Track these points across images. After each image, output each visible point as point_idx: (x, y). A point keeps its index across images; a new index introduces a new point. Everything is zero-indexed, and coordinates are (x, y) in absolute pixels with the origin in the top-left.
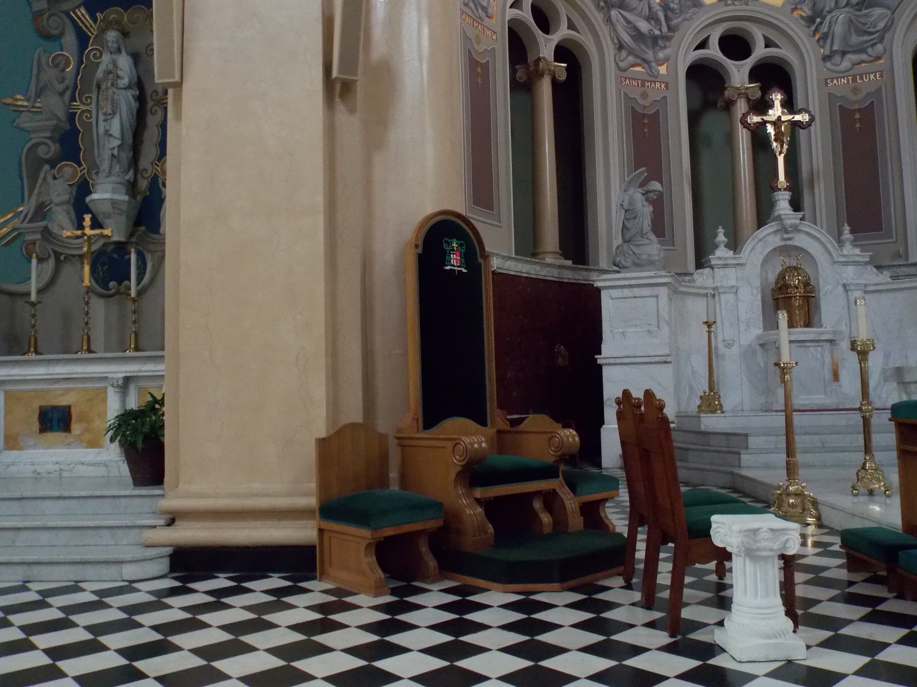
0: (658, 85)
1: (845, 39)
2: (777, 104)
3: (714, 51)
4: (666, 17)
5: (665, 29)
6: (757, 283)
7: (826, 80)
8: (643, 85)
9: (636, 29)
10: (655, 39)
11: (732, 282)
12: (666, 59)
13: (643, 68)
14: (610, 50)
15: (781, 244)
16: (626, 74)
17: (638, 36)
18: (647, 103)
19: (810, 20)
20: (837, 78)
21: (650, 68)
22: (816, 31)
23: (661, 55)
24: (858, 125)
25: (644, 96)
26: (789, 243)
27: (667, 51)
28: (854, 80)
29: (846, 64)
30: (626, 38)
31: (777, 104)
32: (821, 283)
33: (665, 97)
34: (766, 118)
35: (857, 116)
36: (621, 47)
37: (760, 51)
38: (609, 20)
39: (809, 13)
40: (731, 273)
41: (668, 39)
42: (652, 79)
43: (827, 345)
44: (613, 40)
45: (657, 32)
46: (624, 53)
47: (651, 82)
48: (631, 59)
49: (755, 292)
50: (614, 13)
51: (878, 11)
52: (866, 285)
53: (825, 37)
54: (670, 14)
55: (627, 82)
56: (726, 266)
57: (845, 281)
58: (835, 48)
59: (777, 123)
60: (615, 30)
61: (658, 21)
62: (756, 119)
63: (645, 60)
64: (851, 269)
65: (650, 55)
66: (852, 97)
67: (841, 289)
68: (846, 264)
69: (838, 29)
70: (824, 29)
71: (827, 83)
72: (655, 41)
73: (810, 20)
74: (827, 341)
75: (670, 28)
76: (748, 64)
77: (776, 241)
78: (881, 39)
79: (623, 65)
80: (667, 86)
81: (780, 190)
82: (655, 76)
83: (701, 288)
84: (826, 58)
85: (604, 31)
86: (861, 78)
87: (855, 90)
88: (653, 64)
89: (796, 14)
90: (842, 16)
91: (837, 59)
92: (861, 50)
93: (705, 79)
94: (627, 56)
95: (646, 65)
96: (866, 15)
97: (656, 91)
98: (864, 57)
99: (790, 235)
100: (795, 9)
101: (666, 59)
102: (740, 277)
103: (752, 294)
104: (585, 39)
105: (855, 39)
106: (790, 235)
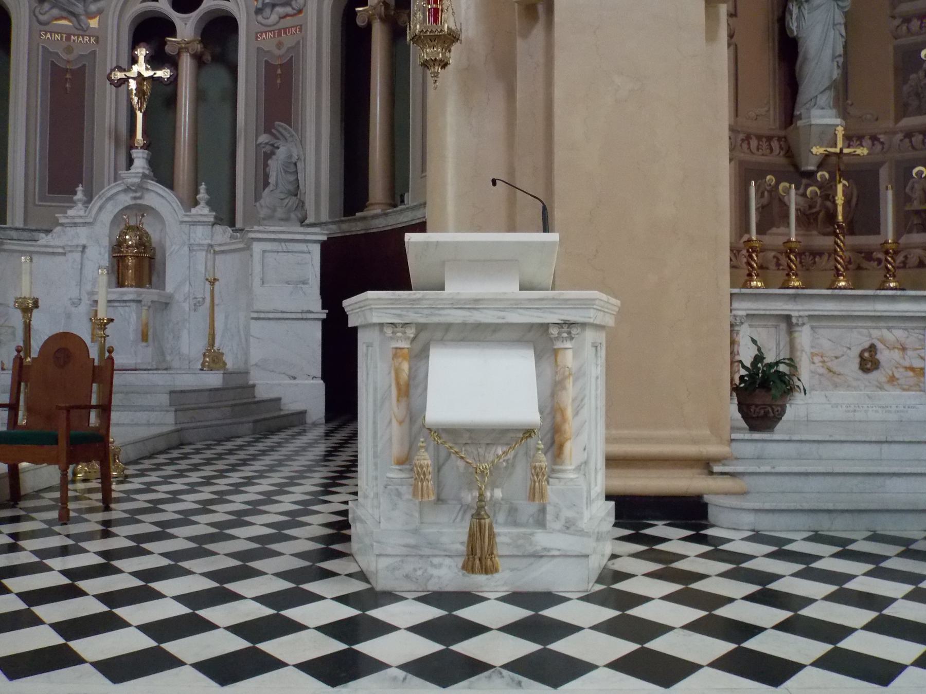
0: (86, 39)
2: (141, 59)
6: (105, 242)
7: (257, 33)
8: (68, 38)
11: (83, 241)
12: (100, 12)
13: (70, 21)
15: (132, 202)
16: (47, 28)
18: (71, 57)
20: (265, 32)
21: (79, 21)
23: (93, 8)
24: (279, 81)
25: (69, 50)
26: (139, 202)
28: (279, 35)
29: (274, 18)
31: (141, 59)
32: (168, 244)
33: (94, 52)
34: (128, 74)
35: (279, 72)
40: (83, 231)
42: (81, 32)
43: (133, 305)
47: (78, 36)
48: (55, 12)
49: (103, 251)
52: (211, 246)
55: (48, 35)
56: (75, 225)
57: (192, 241)
59: (140, 78)
62: (119, 75)
64: (200, 230)
66: (277, 52)
67: (186, 248)
68: (194, 223)
71: (257, 37)
74: (133, 301)
77: (126, 200)
79: (43, 18)
80: (97, 41)
81: (137, 148)
82: (83, 30)
83: (46, 246)
86: (285, 33)
87: (279, 45)
88: (83, 17)
94: (51, 8)
95: (74, 19)
97: (82, 43)
98: (289, 10)
99: (138, 194)
101: (100, 12)
103: (100, 254)
106: (138, 194)
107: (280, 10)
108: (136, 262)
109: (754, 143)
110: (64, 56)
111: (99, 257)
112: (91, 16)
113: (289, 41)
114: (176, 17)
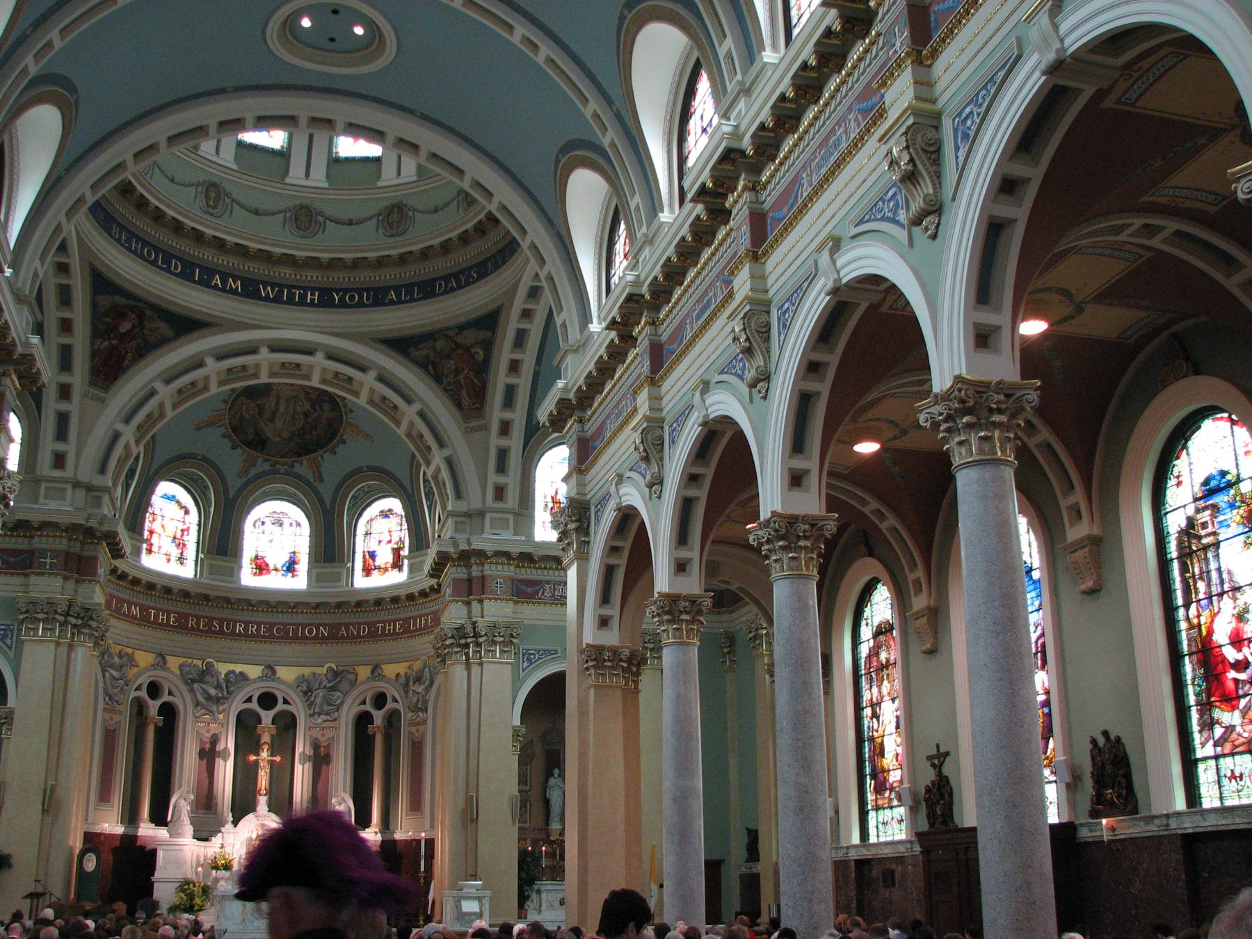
1: (321, 707)
3: (254, 705)
9: (207, 693)
12: (224, 710)
17: (209, 698)
19: (305, 693)
29: (320, 721)
30: (201, 699)
36: (198, 704)
37: (281, 706)
38: (192, 691)
48: (203, 711)
53: (312, 703)
69: (319, 700)
72: (218, 700)
73: (305, 693)
76: (272, 713)
84: (311, 716)
85: (188, 697)
87: (323, 735)
90: (321, 693)
92: (327, 714)
101: (224, 710)
104: (177, 700)
105: (326, 707)
107: (324, 717)
113: (329, 734)
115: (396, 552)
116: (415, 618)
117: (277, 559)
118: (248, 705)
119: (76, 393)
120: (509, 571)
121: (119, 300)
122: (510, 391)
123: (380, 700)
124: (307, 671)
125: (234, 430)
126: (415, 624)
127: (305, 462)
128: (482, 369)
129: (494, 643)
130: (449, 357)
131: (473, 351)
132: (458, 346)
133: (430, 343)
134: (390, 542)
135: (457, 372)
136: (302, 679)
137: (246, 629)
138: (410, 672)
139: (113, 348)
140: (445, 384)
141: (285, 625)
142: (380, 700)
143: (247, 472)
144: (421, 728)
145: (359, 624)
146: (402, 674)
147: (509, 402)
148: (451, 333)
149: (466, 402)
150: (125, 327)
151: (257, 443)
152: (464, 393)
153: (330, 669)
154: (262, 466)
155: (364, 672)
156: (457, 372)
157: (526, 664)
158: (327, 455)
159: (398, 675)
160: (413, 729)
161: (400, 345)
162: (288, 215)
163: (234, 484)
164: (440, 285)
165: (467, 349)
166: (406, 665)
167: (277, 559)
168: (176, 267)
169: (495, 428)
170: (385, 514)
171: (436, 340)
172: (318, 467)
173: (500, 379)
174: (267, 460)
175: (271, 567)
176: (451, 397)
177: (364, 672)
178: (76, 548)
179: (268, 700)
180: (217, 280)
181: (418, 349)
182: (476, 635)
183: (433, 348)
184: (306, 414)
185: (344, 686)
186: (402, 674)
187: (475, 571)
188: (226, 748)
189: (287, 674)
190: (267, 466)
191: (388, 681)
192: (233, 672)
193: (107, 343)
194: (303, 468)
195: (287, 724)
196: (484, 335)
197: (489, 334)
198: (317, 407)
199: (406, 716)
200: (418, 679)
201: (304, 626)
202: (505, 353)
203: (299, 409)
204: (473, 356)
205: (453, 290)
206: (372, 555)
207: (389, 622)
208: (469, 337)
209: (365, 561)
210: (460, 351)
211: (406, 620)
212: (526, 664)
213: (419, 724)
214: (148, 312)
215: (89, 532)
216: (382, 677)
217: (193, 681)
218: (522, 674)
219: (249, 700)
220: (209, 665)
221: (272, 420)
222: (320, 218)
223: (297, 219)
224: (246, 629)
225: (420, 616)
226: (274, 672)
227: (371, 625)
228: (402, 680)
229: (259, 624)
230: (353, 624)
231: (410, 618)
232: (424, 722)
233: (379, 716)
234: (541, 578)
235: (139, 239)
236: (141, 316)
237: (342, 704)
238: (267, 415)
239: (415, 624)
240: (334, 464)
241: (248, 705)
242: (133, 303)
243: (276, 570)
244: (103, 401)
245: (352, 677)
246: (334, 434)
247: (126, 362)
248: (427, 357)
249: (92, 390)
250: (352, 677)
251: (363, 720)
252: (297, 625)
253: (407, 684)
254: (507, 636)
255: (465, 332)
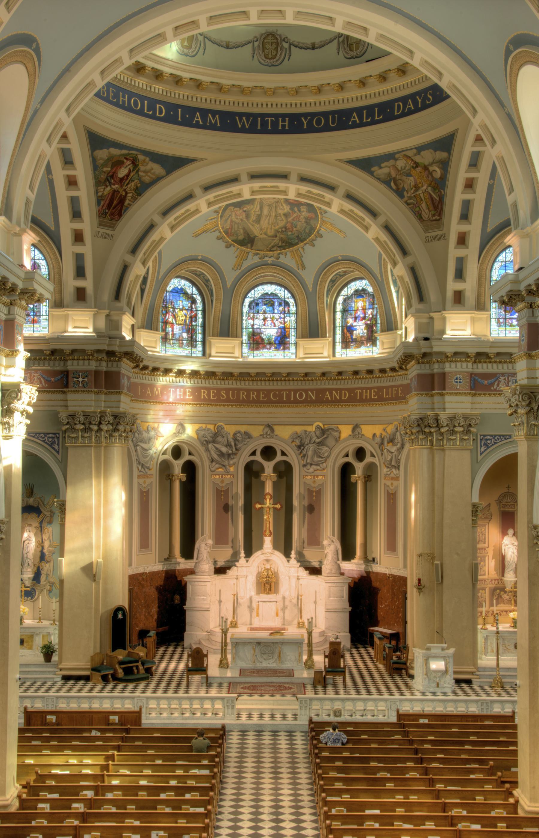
1: (312, 458)
3: (258, 457)
4: (235, 444)
5: (234, 450)
8: (222, 477)
9: (220, 451)
10: (229, 455)
14: (207, 462)
17: (222, 454)
18: (223, 485)
19: (299, 447)
22: (301, 452)
23: (231, 462)
27: (235, 460)
28: (314, 478)
29: (311, 470)
30: (215, 456)
36: (212, 461)
37: (279, 458)
38: (207, 450)
39: (299, 444)
41: (236, 454)
44: (208, 458)
45: (230, 452)
46: (214, 463)
48: (217, 466)
50: (210, 446)
51: (325, 448)
53: (304, 456)
54: (237, 442)
58: (308, 461)
60: (210, 454)
61: (231, 446)
63: (224, 466)
64: (293, 569)
65: (226, 463)
68: (290, 567)
69: (310, 453)
70: (304, 452)
73: (299, 447)
75: (237, 450)
77: (263, 557)
78: (325, 461)
79: (213, 469)
82: (227, 472)
84: (304, 466)
89: (293, 444)
90: (312, 447)
91: (308, 466)
92: (317, 465)
93: (252, 472)
96: (321, 449)
98: (318, 467)
100: (293, 441)
101: (234, 464)
102: (247, 571)
105: (316, 459)
108: (268, 584)
109: (493, 581)
110: (221, 485)
111: (252, 579)
112: (230, 466)
114: (265, 463)
115: (370, 328)
116: (387, 388)
117: (270, 332)
118: (253, 458)
119: (88, 236)
120: (467, 367)
121: (115, 151)
122: (467, 205)
123: (360, 453)
124: (299, 429)
125: (226, 232)
126: (387, 394)
127: (288, 253)
128: (440, 185)
129: (453, 432)
130: (409, 175)
131: (431, 169)
132: (417, 165)
133: (392, 162)
134: (364, 318)
135: (417, 188)
136: (296, 436)
137: (248, 396)
138: (384, 434)
139: (115, 192)
140: (406, 199)
141: (280, 391)
142: (360, 453)
143: (240, 265)
144: (395, 483)
145: (341, 390)
146: (378, 434)
147: (465, 217)
148: (410, 154)
149: (426, 214)
150: (122, 172)
151: (248, 241)
152: (424, 205)
153: (318, 427)
154: (253, 260)
155: (346, 431)
156: (417, 188)
157: (483, 449)
158: (307, 247)
159: (374, 435)
160: (389, 483)
161: (365, 165)
162: (256, 44)
163: (230, 279)
164: (399, 106)
165: (426, 168)
166: (382, 427)
167: (270, 332)
168: (161, 112)
169: (453, 239)
170: (360, 293)
171: (396, 160)
172: (301, 257)
173: (457, 197)
174: (257, 254)
175: (266, 341)
176: (412, 210)
177: (346, 431)
178: (104, 367)
179: (268, 452)
180: (198, 117)
181: (381, 168)
182: (438, 426)
183: (394, 166)
184: (286, 215)
185: (330, 441)
186: (378, 434)
187: (436, 368)
188: (237, 493)
189: (284, 432)
190: (256, 259)
191: (367, 440)
192: (239, 432)
193: (109, 189)
194: (287, 259)
195: (285, 472)
196: (441, 155)
197: (444, 155)
198: (296, 209)
199: (383, 470)
200: (392, 441)
201: (296, 391)
202: (461, 173)
203: (280, 212)
204: (431, 173)
205: (411, 112)
206: (350, 329)
207: (366, 389)
208: (427, 157)
209: (343, 334)
210: (419, 169)
211: (380, 389)
212: (483, 449)
213: (392, 479)
214: (141, 157)
215: (111, 354)
216: (361, 436)
217: (208, 442)
218: (480, 458)
219: (254, 453)
220: (220, 428)
221: (258, 220)
222: (286, 45)
223: (264, 49)
224: (248, 396)
225: (392, 387)
226: (272, 430)
227: (351, 391)
228: (378, 440)
229: (258, 391)
230: (336, 390)
231: (383, 387)
232: (397, 478)
233: (359, 468)
234: (495, 371)
235: (125, 91)
236: (135, 162)
237: (328, 457)
238: (253, 218)
239: (387, 394)
240: (314, 255)
241: (253, 458)
242: (124, 152)
243: (270, 343)
244: (111, 237)
245: (336, 434)
246: (312, 229)
247: (127, 202)
248: (389, 174)
249: (103, 230)
250: (336, 434)
251: (346, 470)
252: (290, 390)
253: (382, 444)
254: (467, 425)
255: (422, 153)
